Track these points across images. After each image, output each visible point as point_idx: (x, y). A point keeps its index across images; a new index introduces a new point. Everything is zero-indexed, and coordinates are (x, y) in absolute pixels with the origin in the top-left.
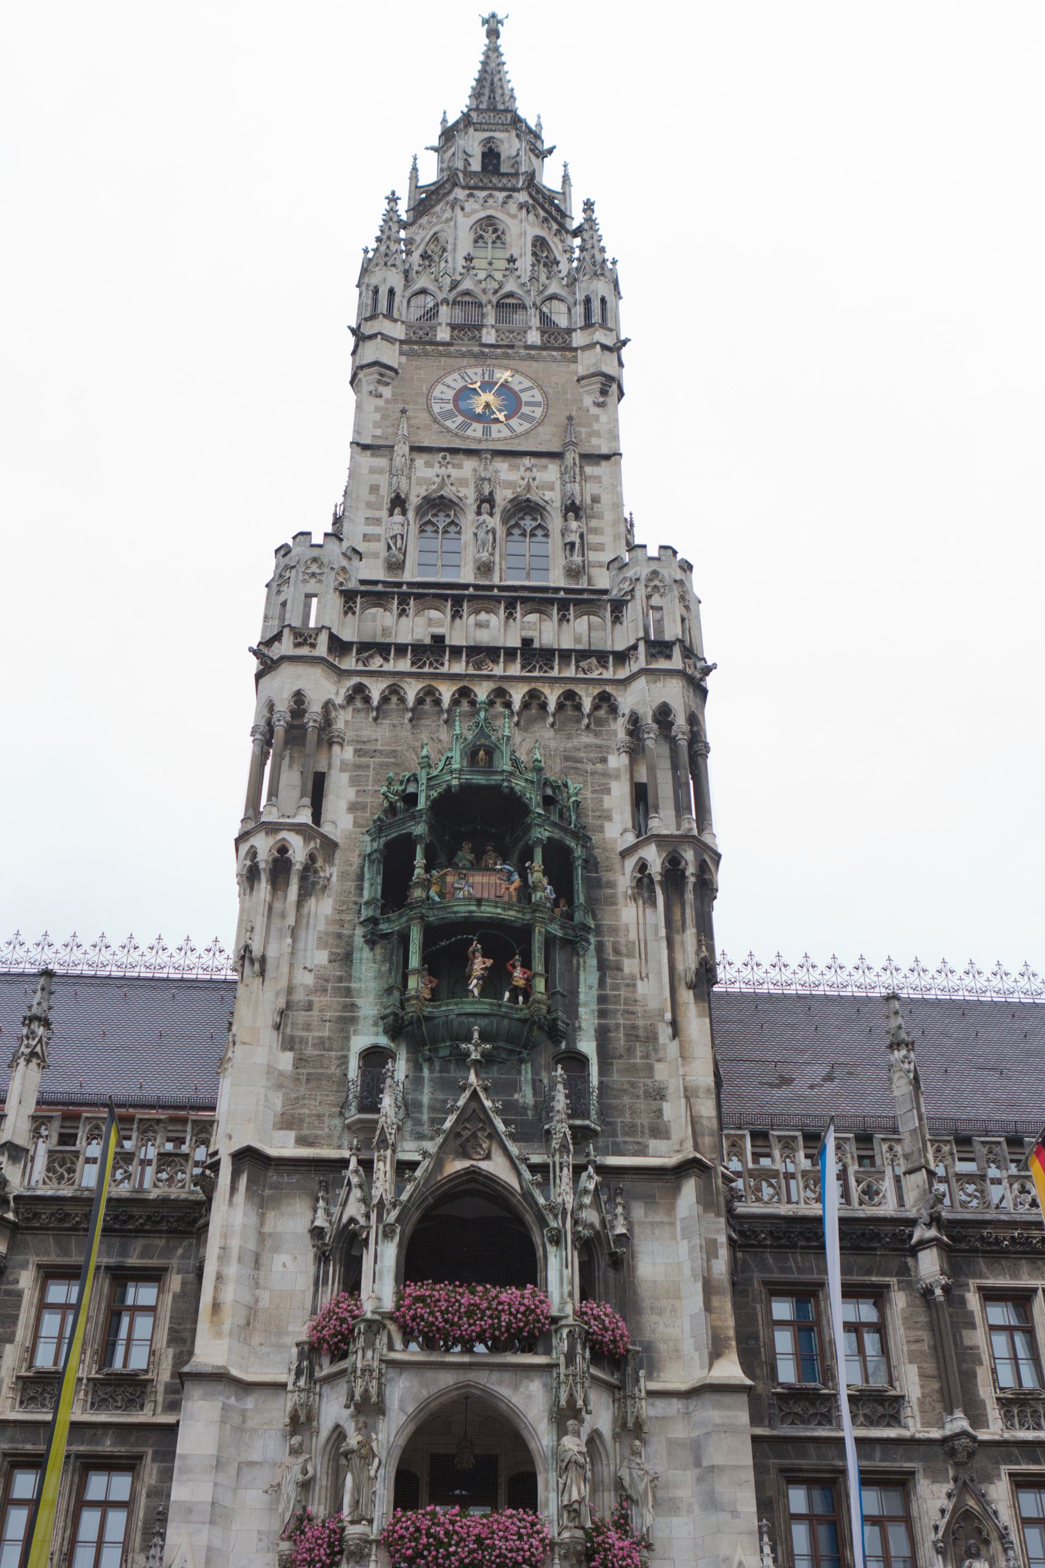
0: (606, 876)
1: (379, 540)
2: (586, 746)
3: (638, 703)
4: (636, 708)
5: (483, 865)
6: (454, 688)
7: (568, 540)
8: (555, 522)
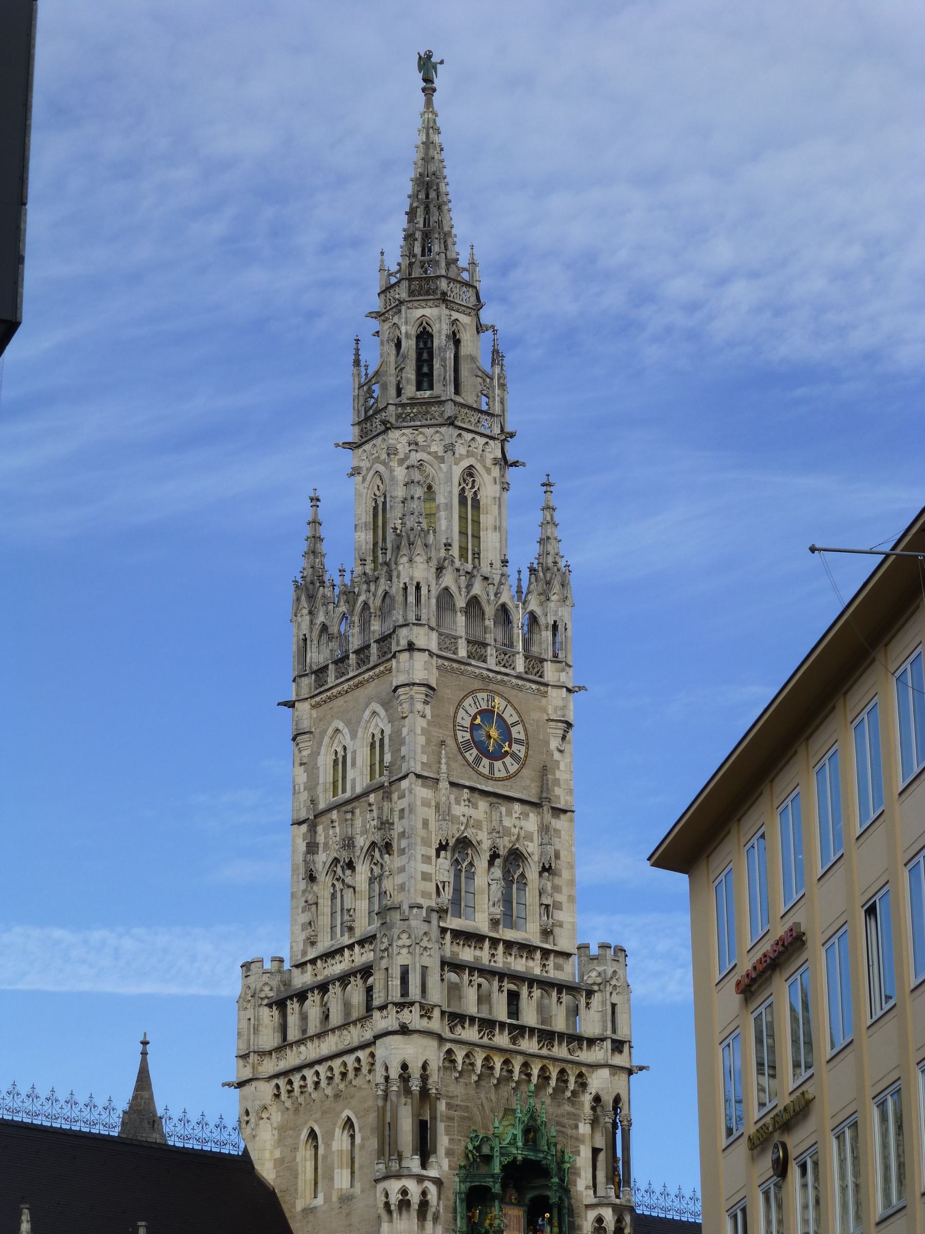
0: (578, 1221)
1: (431, 880)
2: (569, 1114)
3: (602, 1089)
4: (601, 1093)
5: (508, 1200)
6: (502, 1060)
7: (545, 901)
8: (532, 873)
